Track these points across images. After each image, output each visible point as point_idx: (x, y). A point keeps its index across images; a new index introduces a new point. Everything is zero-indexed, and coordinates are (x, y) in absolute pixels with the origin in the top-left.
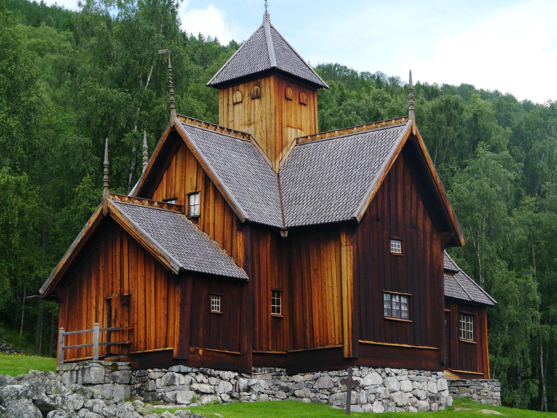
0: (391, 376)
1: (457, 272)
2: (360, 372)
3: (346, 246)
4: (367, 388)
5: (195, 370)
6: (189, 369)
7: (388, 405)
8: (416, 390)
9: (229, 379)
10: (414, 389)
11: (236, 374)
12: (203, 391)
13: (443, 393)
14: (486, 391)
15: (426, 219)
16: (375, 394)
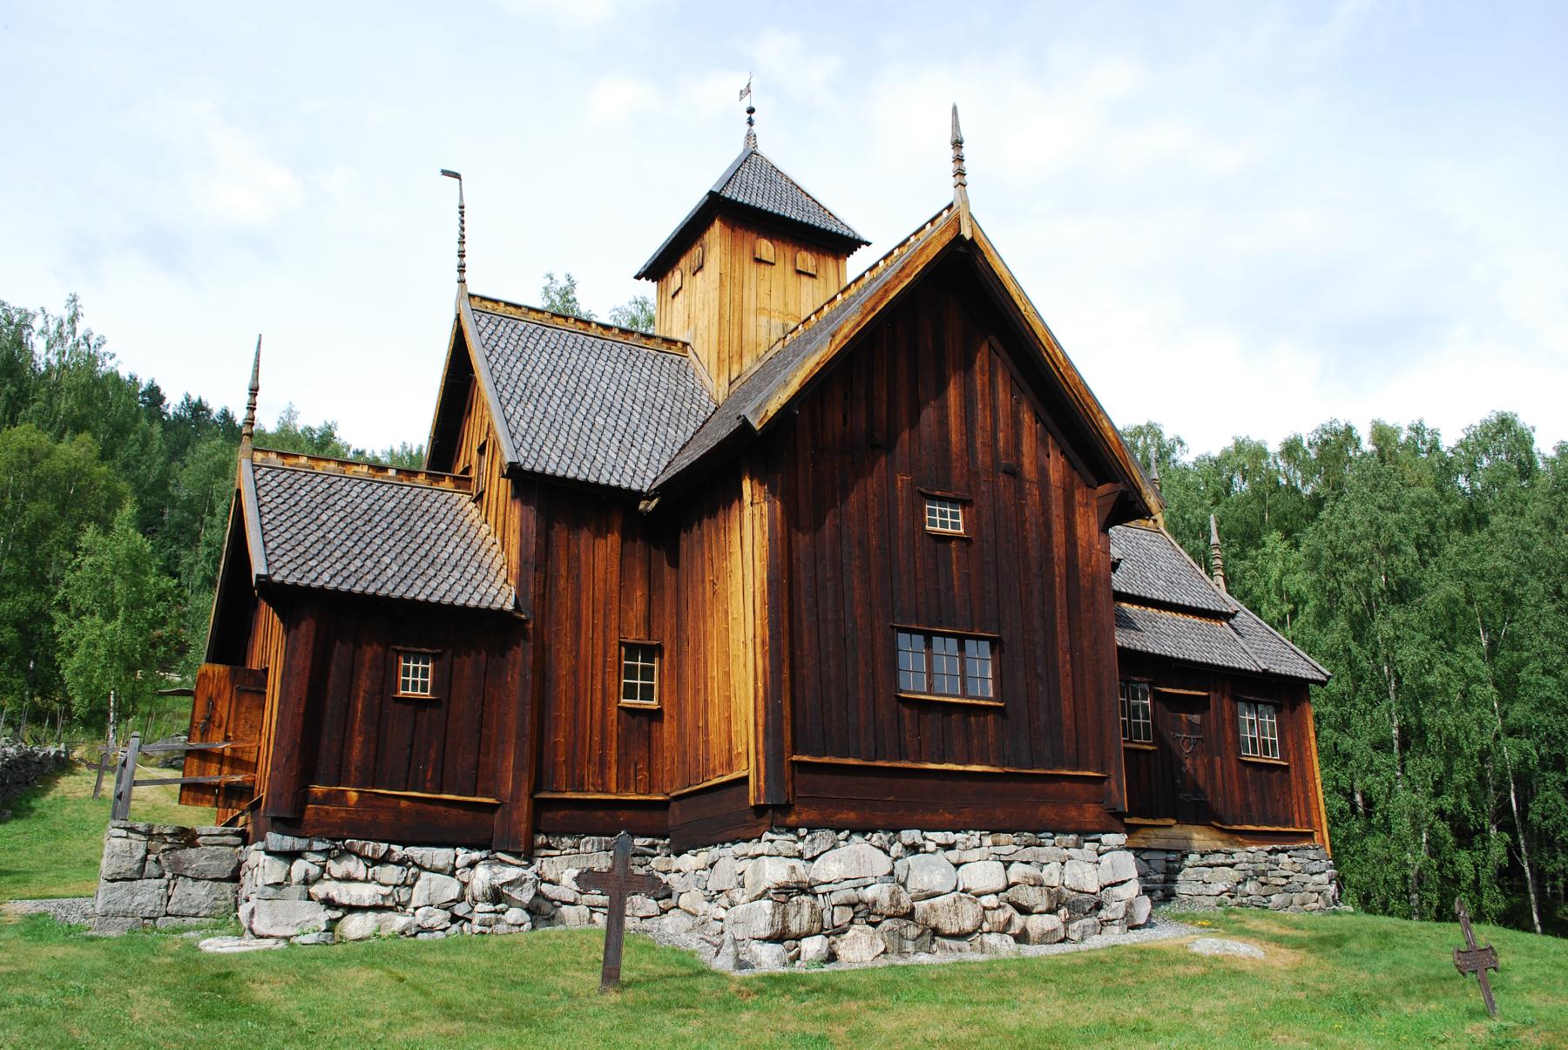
0: (925, 852)
1: (1233, 616)
2: (800, 846)
3: (752, 504)
4: (824, 889)
5: (318, 845)
6: (299, 844)
7: (901, 936)
8: (1017, 887)
9: (449, 869)
10: (1008, 887)
11: (476, 855)
12: (346, 901)
13: (1117, 890)
14: (1285, 873)
15: (1048, 456)
16: (853, 905)
